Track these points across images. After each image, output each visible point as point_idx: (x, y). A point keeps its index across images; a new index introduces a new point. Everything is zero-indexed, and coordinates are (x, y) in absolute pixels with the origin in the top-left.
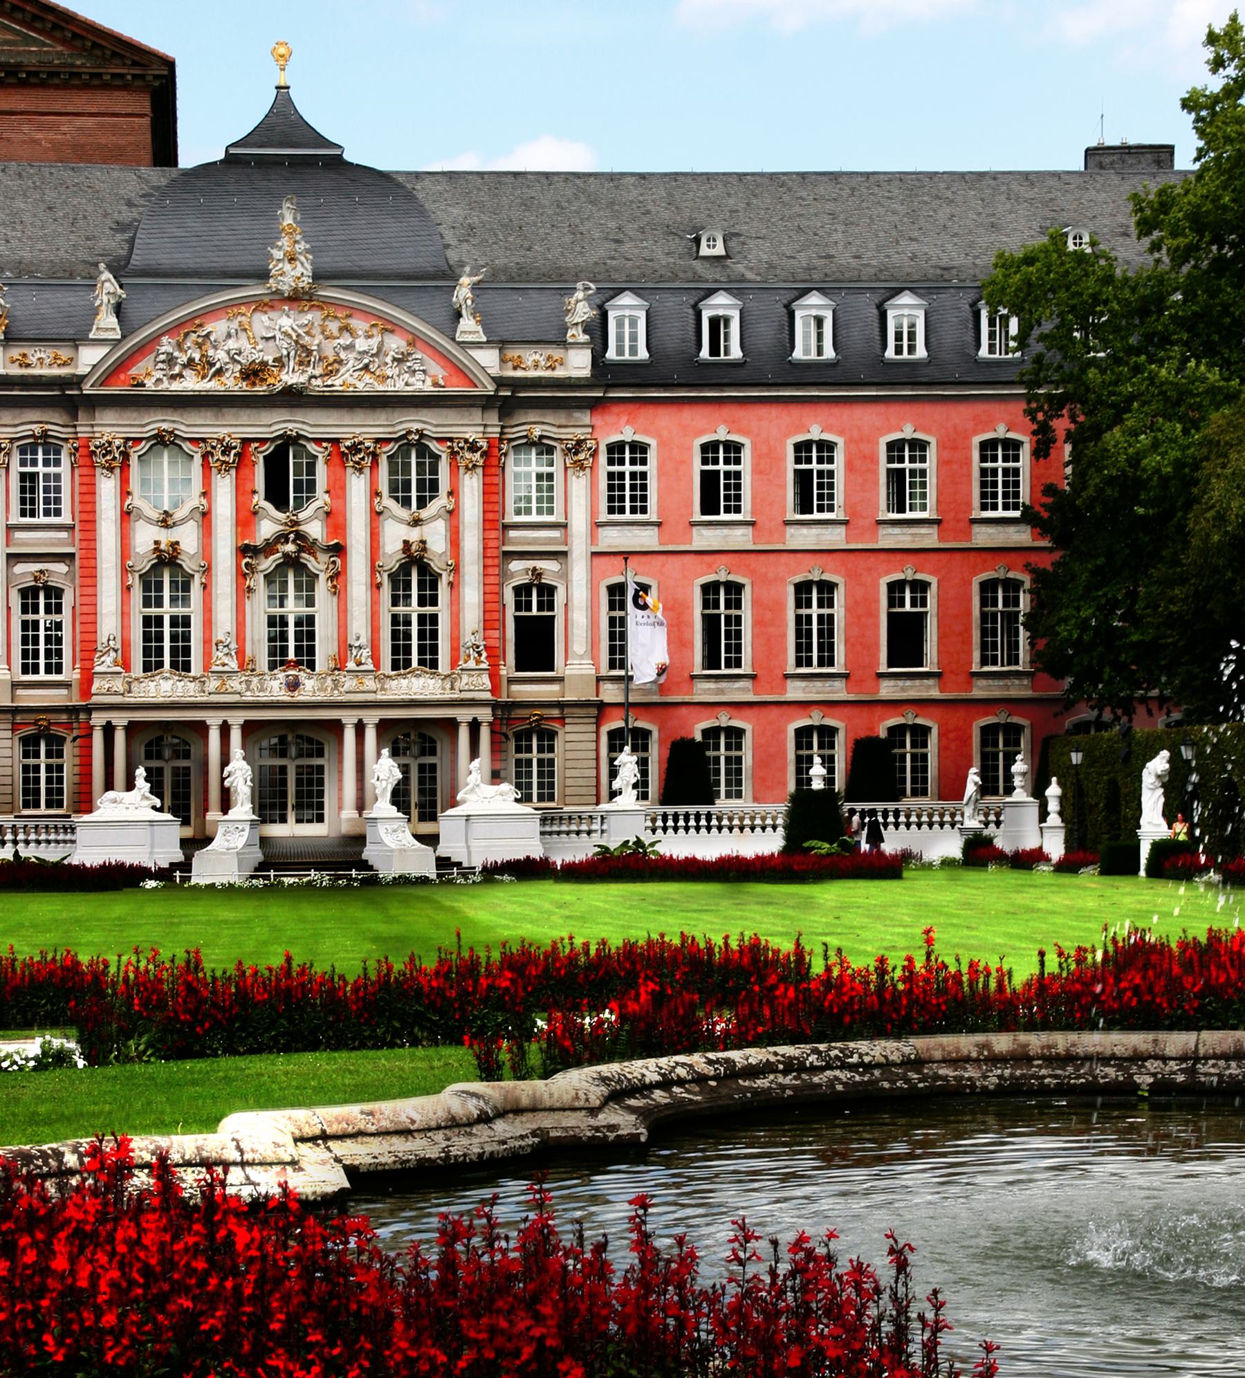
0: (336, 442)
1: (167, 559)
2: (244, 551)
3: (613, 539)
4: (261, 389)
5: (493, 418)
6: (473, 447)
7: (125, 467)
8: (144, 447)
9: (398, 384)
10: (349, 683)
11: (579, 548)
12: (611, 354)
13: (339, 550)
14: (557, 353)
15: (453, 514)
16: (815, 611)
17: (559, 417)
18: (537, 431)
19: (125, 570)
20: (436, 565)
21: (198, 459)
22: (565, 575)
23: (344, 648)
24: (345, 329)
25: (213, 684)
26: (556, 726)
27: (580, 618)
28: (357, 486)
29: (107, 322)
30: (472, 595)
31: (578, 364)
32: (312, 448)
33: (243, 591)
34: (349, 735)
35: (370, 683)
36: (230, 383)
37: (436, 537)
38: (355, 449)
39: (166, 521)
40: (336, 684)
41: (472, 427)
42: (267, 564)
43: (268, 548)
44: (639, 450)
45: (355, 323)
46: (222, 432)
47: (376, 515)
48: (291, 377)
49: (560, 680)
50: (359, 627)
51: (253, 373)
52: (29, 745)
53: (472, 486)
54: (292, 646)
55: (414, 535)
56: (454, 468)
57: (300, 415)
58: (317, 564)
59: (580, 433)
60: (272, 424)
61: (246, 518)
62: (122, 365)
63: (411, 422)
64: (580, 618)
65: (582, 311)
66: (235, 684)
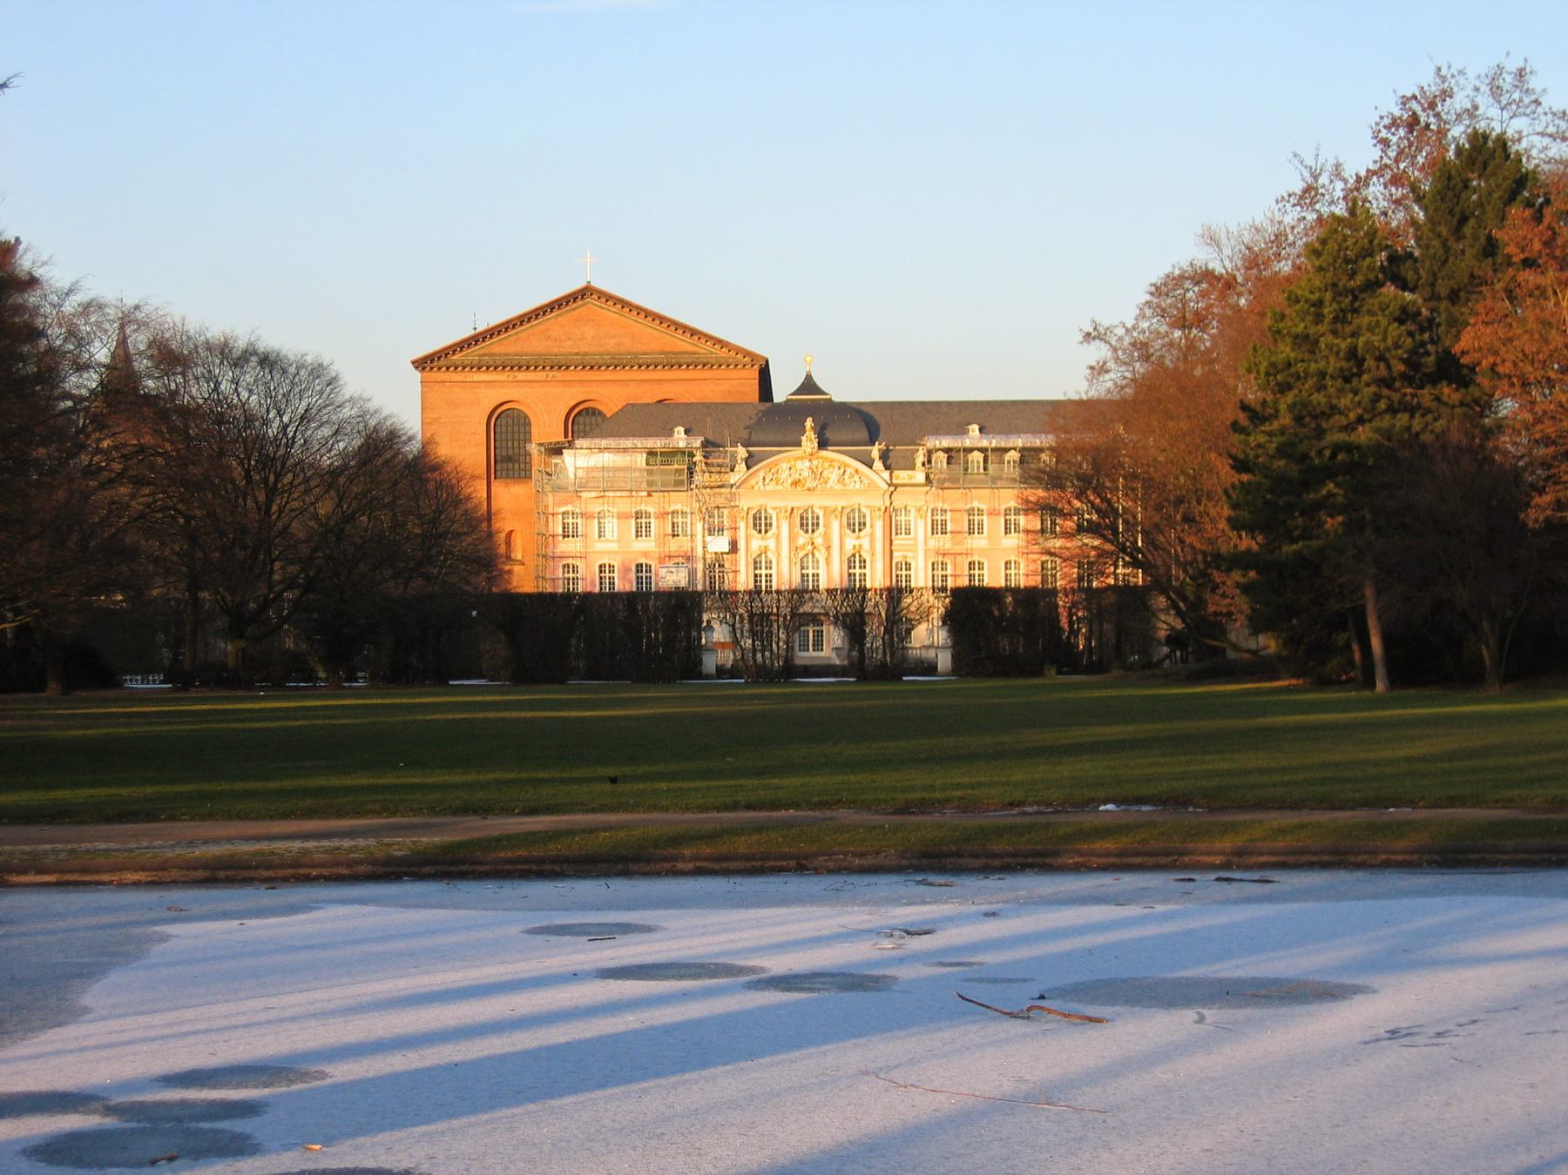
0: (825, 509)
11: (921, 548)
13: (828, 548)
16: (1013, 572)
28: (835, 525)
30: (879, 566)
31: (920, 476)
46: (782, 504)
48: (809, 484)
51: (796, 483)
53: (879, 525)
55: (857, 543)
58: (821, 556)
61: (792, 539)
65: (920, 458)
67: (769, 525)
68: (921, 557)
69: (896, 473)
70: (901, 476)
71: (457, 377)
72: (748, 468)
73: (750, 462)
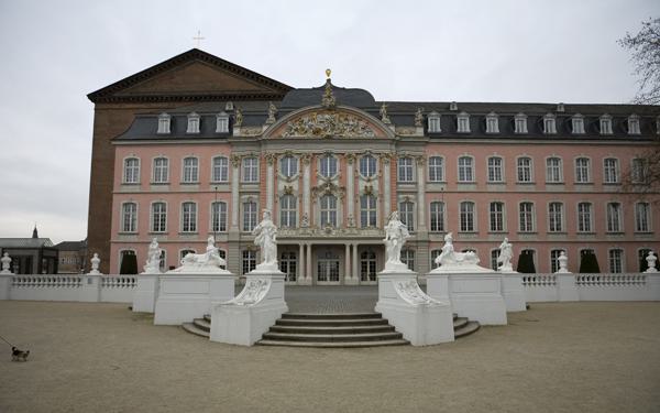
1: (288, 192)
2: (314, 189)
3: (431, 187)
4: (319, 137)
5: (393, 147)
6: (387, 156)
7: (276, 163)
8: (282, 157)
9: (365, 135)
10: (348, 231)
11: (421, 190)
12: (429, 130)
13: (344, 189)
14: (413, 129)
15: (381, 178)
17: (414, 148)
18: (407, 153)
19: (275, 196)
20: (376, 194)
21: (298, 162)
22: (417, 199)
23: (346, 218)
24: (346, 119)
25: (301, 231)
26: (414, 249)
27: (422, 213)
28: (350, 169)
29: (272, 118)
31: (420, 132)
32: (335, 157)
33: (313, 203)
34: (348, 250)
35: (356, 232)
36: (309, 135)
37: (375, 185)
38: (350, 156)
39: (288, 181)
40: (344, 231)
41: (387, 149)
42: (321, 194)
43: (321, 188)
44: (439, 159)
45: (350, 118)
47: (356, 178)
49: (415, 234)
50: (351, 212)
51: (317, 132)
52: (245, 254)
53: (387, 169)
54: (328, 220)
55: (368, 185)
56: (381, 167)
57: (333, 146)
59: (421, 153)
60: (322, 148)
61: (314, 178)
62: (276, 130)
63: (366, 148)
64: (422, 213)
65: (420, 117)
66: (309, 231)
67: (293, 170)
68: (421, 198)
69: (400, 128)
70: (406, 132)
71: (117, 106)
72: (277, 119)
73: (277, 116)
